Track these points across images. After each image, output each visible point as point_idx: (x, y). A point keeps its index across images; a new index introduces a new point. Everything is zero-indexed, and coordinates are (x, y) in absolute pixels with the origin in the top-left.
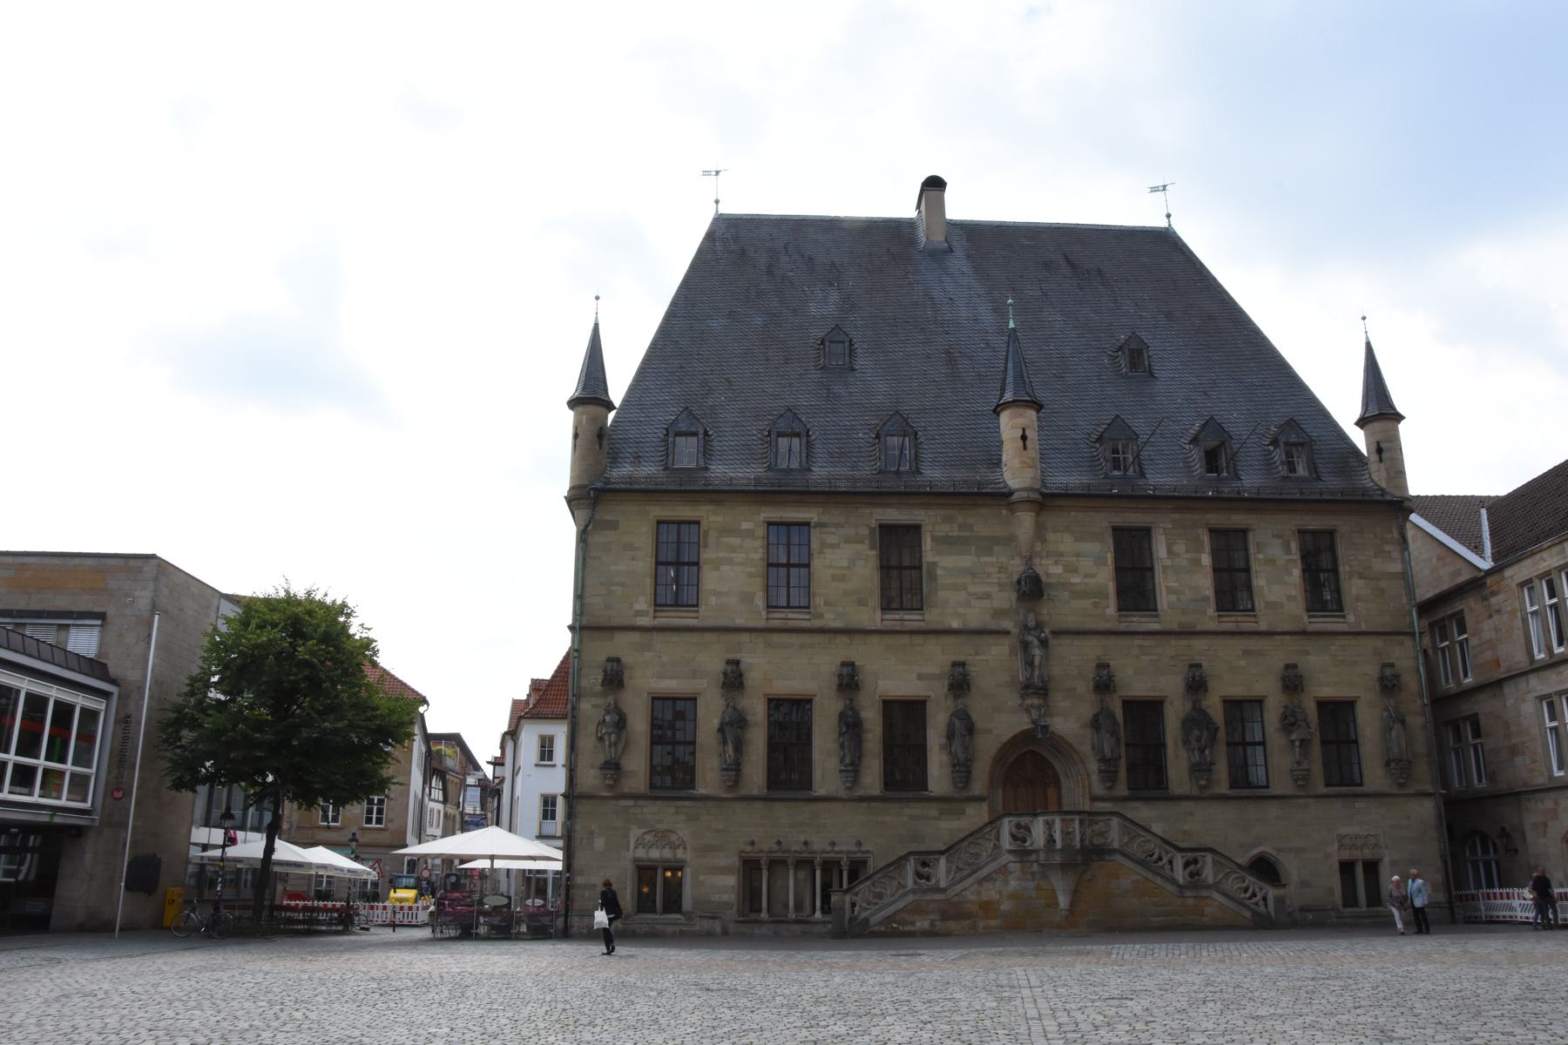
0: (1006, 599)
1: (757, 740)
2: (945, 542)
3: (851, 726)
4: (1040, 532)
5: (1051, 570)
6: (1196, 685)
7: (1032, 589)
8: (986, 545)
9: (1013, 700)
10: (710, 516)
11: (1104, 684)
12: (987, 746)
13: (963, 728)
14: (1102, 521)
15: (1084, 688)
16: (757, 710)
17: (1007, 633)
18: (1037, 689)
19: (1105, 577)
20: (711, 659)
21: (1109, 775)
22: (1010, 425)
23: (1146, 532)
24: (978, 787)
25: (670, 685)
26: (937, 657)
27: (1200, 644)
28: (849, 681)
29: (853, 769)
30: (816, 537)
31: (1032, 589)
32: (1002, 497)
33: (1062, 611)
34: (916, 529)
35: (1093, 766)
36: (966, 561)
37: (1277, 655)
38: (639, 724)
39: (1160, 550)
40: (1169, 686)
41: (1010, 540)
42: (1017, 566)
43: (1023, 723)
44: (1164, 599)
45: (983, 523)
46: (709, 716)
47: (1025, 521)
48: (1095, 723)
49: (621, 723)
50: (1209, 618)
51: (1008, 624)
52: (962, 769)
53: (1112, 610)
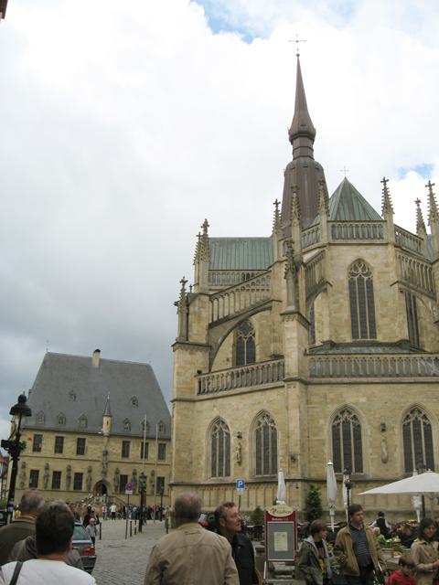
0: (100, 454)
1: (51, 479)
2: (90, 442)
3: (69, 478)
4: (108, 441)
5: (110, 449)
6: (135, 474)
7: (106, 453)
8: (98, 443)
9: (99, 474)
10: (45, 435)
11: (117, 473)
12: (94, 483)
13: (90, 479)
14: (121, 440)
15: (113, 472)
16: (51, 473)
17: (98, 461)
18: (105, 473)
19: (120, 451)
20: (43, 463)
21: (116, 490)
22: (105, 420)
23: (129, 442)
24: (92, 490)
25: (35, 468)
26: (86, 465)
27: (137, 465)
28: (69, 469)
29: (68, 486)
30: (65, 440)
31: (106, 453)
32: (102, 435)
33: (111, 458)
34: (84, 440)
35: (113, 488)
36: (93, 446)
37: (150, 469)
38: (28, 475)
39: (131, 446)
40: (129, 473)
41: (102, 443)
42: (104, 449)
43: (100, 479)
44: (131, 456)
45: (98, 439)
46: (41, 475)
47: (106, 440)
48: (114, 479)
49: (25, 475)
50: (139, 460)
51: (100, 459)
52: (89, 487)
53: (120, 457)
